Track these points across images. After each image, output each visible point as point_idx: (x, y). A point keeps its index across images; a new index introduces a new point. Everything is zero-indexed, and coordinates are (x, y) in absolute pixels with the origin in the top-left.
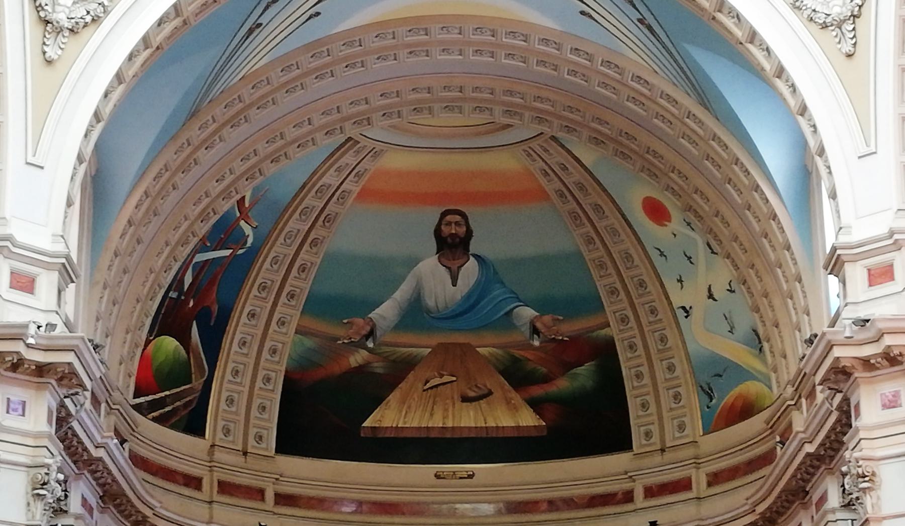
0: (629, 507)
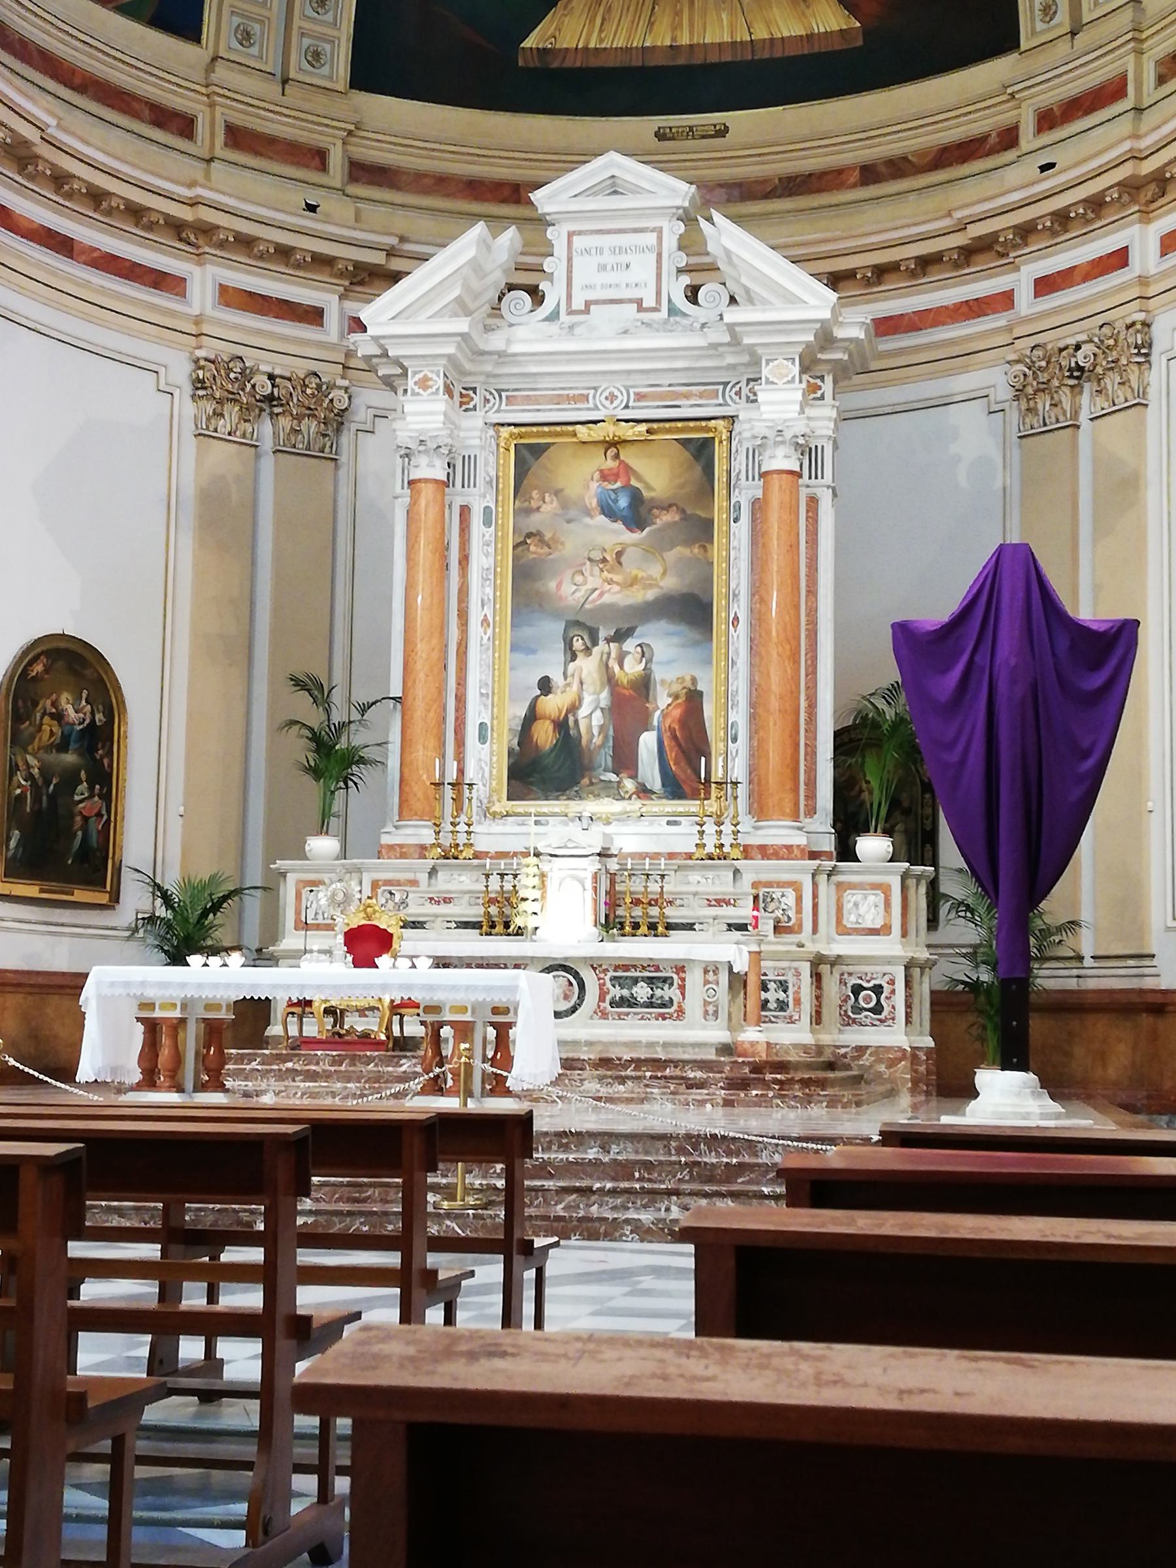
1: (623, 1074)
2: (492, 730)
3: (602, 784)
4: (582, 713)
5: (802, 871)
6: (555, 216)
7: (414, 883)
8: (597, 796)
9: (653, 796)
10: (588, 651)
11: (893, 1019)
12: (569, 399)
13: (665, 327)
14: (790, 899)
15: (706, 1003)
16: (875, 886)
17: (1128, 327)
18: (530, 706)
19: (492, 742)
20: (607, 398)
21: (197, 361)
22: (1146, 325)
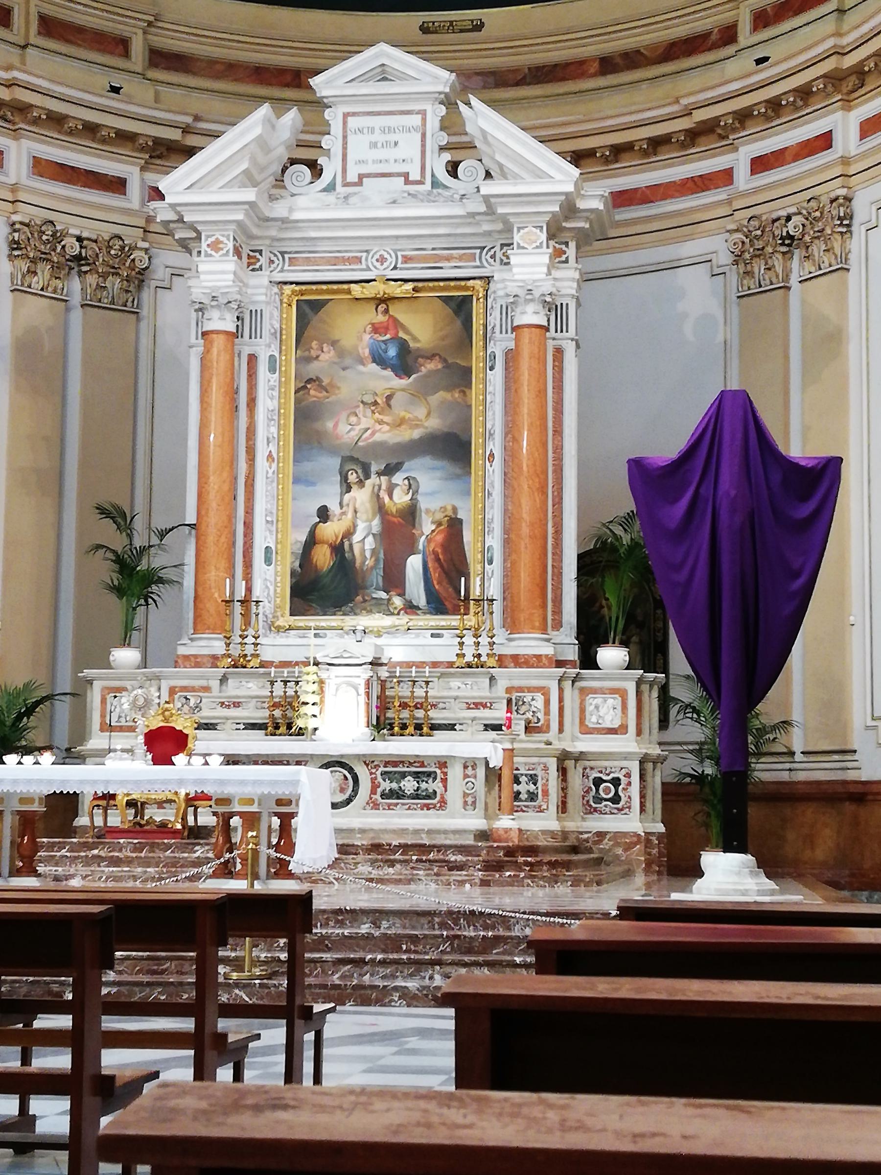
0: (730, 50)
1: (392, 857)
2: (277, 553)
3: (374, 602)
4: (357, 538)
5: (550, 677)
6: (331, 99)
7: (207, 689)
8: (370, 612)
9: (419, 612)
10: (361, 483)
11: (629, 808)
12: (345, 260)
13: (429, 198)
14: (539, 702)
15: (465, 795)
16: (614, 691)
17: (832, 201)
18: (310, 531)
19: (276, 565)
20: (377, 260)
21: (13, 224)
22: (848, 199)
